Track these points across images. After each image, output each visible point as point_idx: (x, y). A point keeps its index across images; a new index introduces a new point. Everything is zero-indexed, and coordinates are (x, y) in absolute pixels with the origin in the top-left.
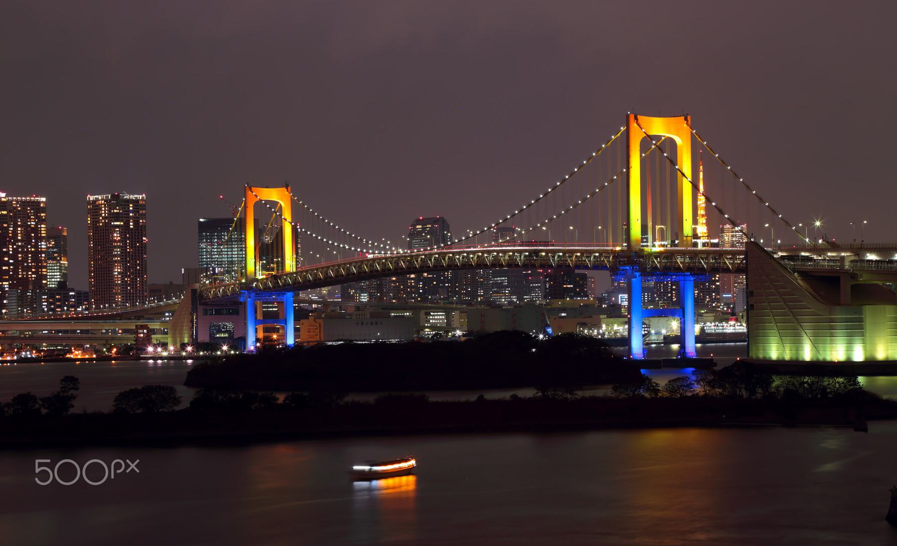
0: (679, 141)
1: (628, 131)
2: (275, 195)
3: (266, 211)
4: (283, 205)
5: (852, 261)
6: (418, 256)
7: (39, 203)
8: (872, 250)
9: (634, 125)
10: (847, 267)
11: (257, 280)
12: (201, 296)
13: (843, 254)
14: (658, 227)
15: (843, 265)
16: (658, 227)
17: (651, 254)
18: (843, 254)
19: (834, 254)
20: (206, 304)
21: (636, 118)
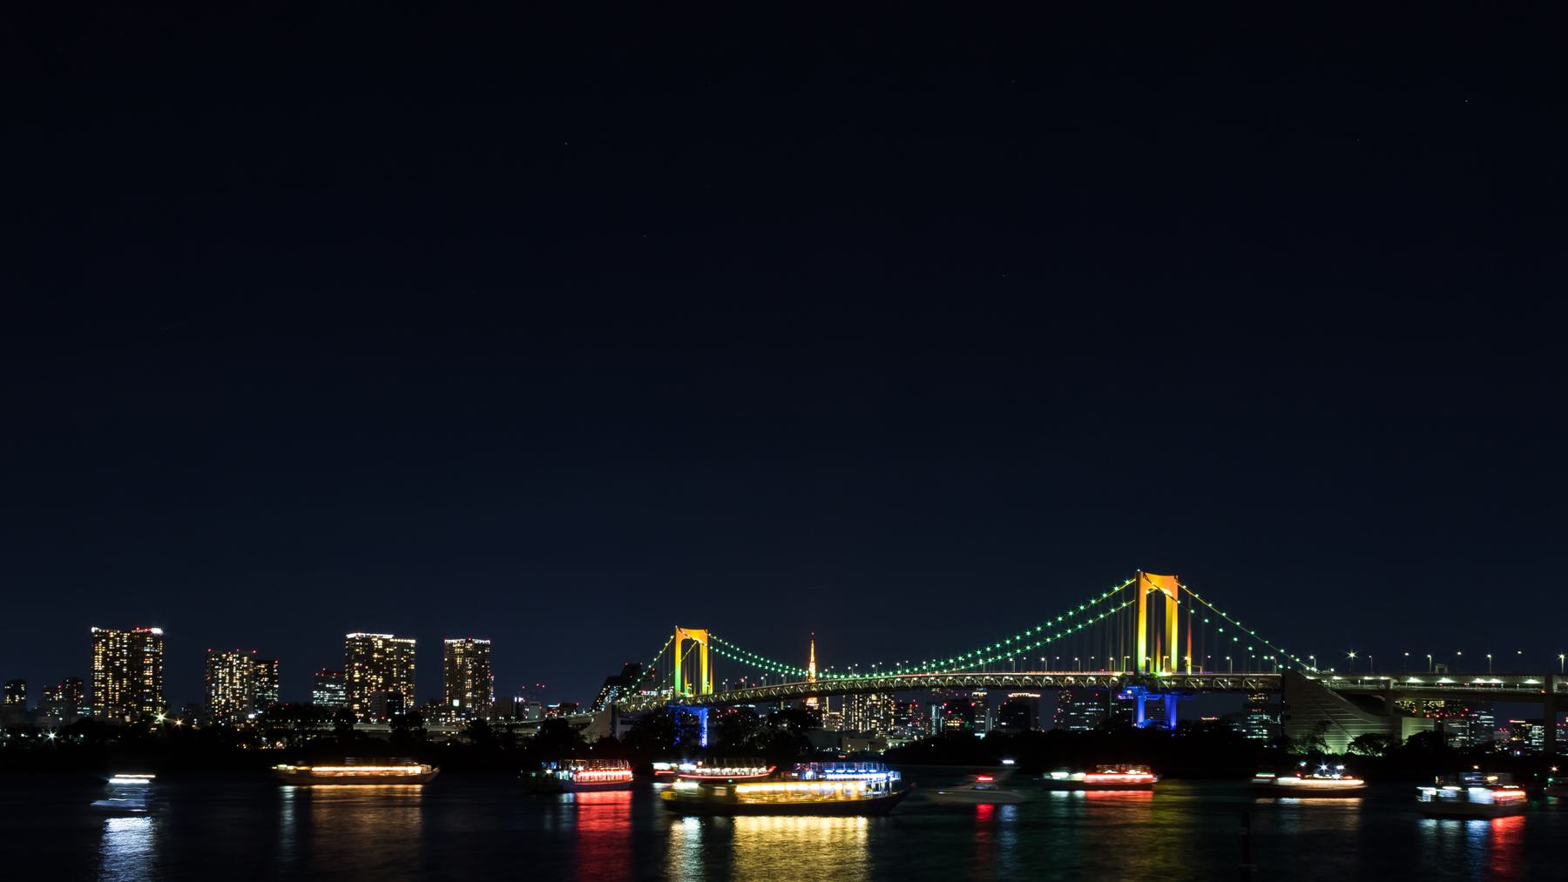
0: (1166, 592)
1: (1138, 582)
2: (699, 636)
3: (690, 646)
4: (700, 642)
5: (1395, 684)
6: (878, 679)
7: (410, 644)
8: (1414, 675)
9: (1143, 580)
10: (1391, 687)
11: (685, 698)
12: (619, 711)
13: (1382, 678)
14: (1165, 657)
15: (1389, 686)
16: (1165, 657)
17: (1159, 678)
18: (1382, 678)
19: (1371, 678)
20: (621, 716)
21: (1144, 575)
